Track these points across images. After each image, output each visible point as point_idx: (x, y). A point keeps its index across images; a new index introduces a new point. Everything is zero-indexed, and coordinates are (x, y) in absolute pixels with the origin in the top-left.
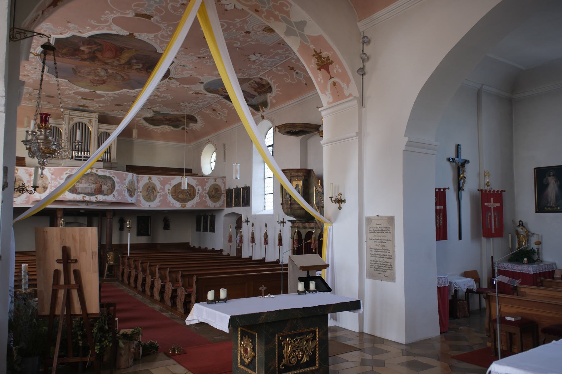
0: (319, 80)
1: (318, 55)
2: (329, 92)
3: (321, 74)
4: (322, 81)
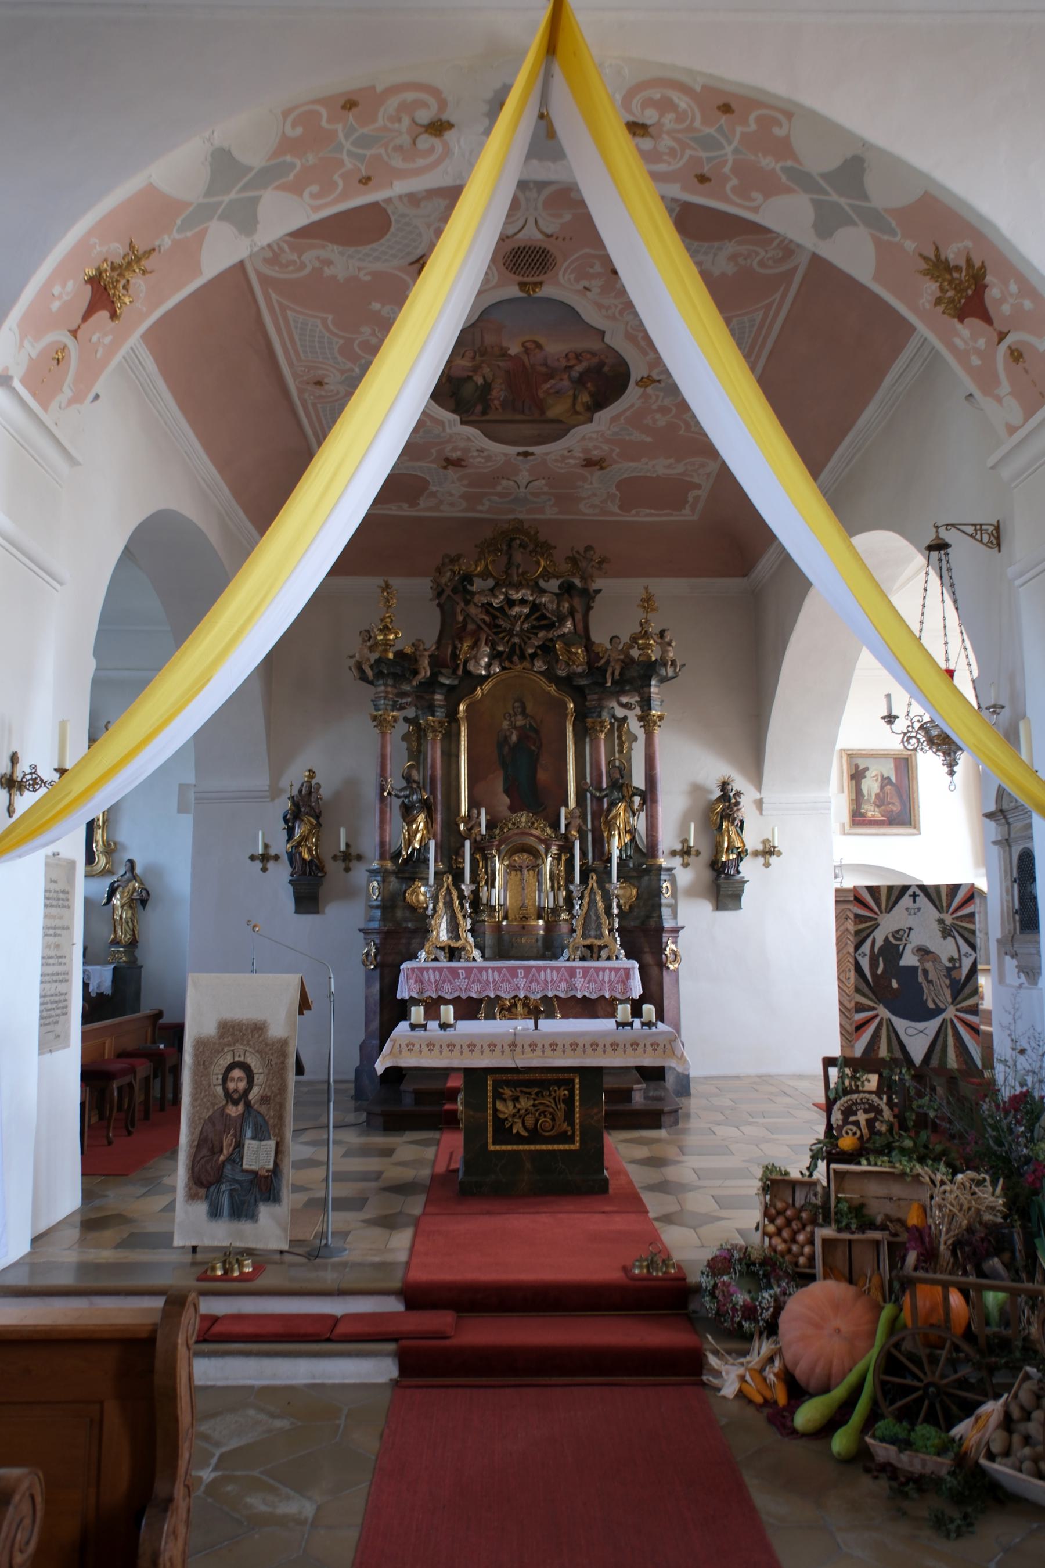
2: (33, 349)
3: (73, 292)
4: (56, 305)
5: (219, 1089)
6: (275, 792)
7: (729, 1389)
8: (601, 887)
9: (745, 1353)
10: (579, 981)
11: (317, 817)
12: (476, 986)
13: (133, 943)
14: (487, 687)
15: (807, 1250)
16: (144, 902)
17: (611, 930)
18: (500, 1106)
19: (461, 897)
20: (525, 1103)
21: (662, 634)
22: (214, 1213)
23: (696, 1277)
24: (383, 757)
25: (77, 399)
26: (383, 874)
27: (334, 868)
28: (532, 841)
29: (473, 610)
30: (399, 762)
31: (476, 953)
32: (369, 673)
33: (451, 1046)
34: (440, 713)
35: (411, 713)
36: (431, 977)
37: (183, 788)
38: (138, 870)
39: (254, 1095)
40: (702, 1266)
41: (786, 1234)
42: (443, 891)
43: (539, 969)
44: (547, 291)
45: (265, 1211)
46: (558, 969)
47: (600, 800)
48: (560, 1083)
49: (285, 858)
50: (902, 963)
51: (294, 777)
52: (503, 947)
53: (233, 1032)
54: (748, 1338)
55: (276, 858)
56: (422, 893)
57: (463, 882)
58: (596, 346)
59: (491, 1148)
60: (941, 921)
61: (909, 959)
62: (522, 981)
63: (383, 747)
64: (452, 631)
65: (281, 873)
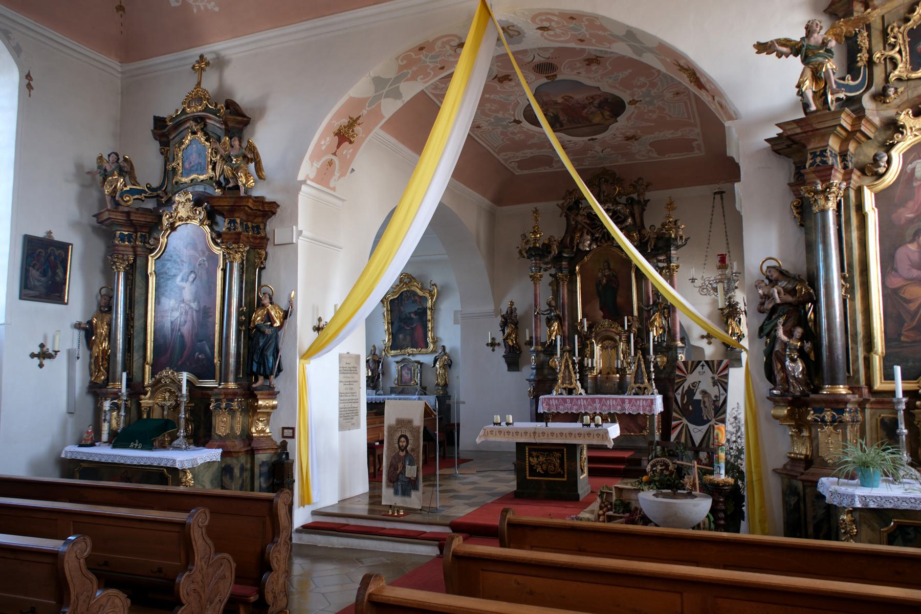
0: (323, 143)
1: (353, 123)
2: (317, 165)
4: (323, 148)
6: (497, 311)
8: (644, 357)
10: (627, 406)
11: (516, 324)
12: (575, 407)
13: (446, 385)
14: (589, 256)
16: (450, 366)
17: (649, 379)
18: (531, 459)
19: (574, 363)
20: (541, 459)
21: (676, 221)
22: (396, 493)
24: (536, 295)
25: (343, 175)
26: (537, 352)
27: (524, 348)
28: (613, 335)
29: (579, 218)
30: (545, 296)
31: (582, 391)
32: (525, 255)
33: (508, 432)
34: (565, 272)
35: (553, 271)
36: (554, 402)
37: (456, 312)
38: (447, 351)
39: (409, 448)
42: (564, 361)
43: (606, 399)
44: (559, 77)
45: (413, 493)
46: (616, 399)
47: (649, 311)
48: (557, 451)
49: (503, 344)
50: (695, 398)
51: (505, 308)
52: (599, 387)
55: (499, 344)
56: (557, 362)
57: (574, 355)
58: (599, 93)
59: (528, 478)
60: (713, 378)
61: (698, 396)
62: (598, 405)
63: (535, 290)
64: (571, 230)
65: (501, 351)
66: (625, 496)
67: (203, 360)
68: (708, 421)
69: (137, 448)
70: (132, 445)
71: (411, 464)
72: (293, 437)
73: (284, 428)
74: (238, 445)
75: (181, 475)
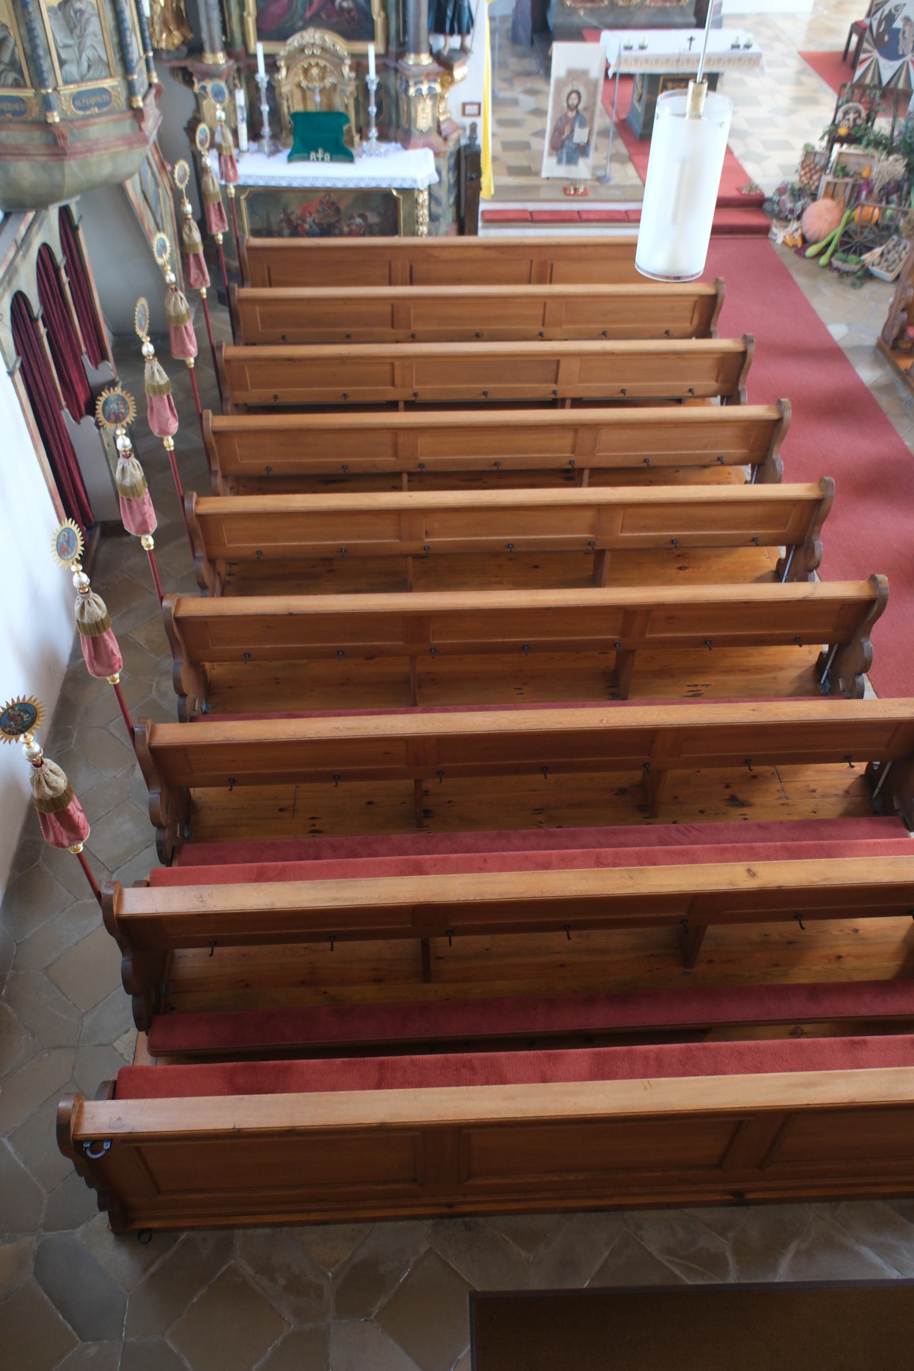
5: (565, 104)
7: (779, 240)
9: (786, 227)
15: (816, 183)
22: (559, 161)
23: (769, 193)
33: (647, 61)
39: (581, 107)
40: (773, 190)
41: (808, 175)
53: (574, 74)
54: (790, 221)
66: (843, 159)
67: (349, 11)
68: (903, 55)
69: (323, 159)
70: (313, 155)
71: (582, 125)
72: (479, 114)
73: (464, 105)
74: (436, 139)
75: (416, 193)
